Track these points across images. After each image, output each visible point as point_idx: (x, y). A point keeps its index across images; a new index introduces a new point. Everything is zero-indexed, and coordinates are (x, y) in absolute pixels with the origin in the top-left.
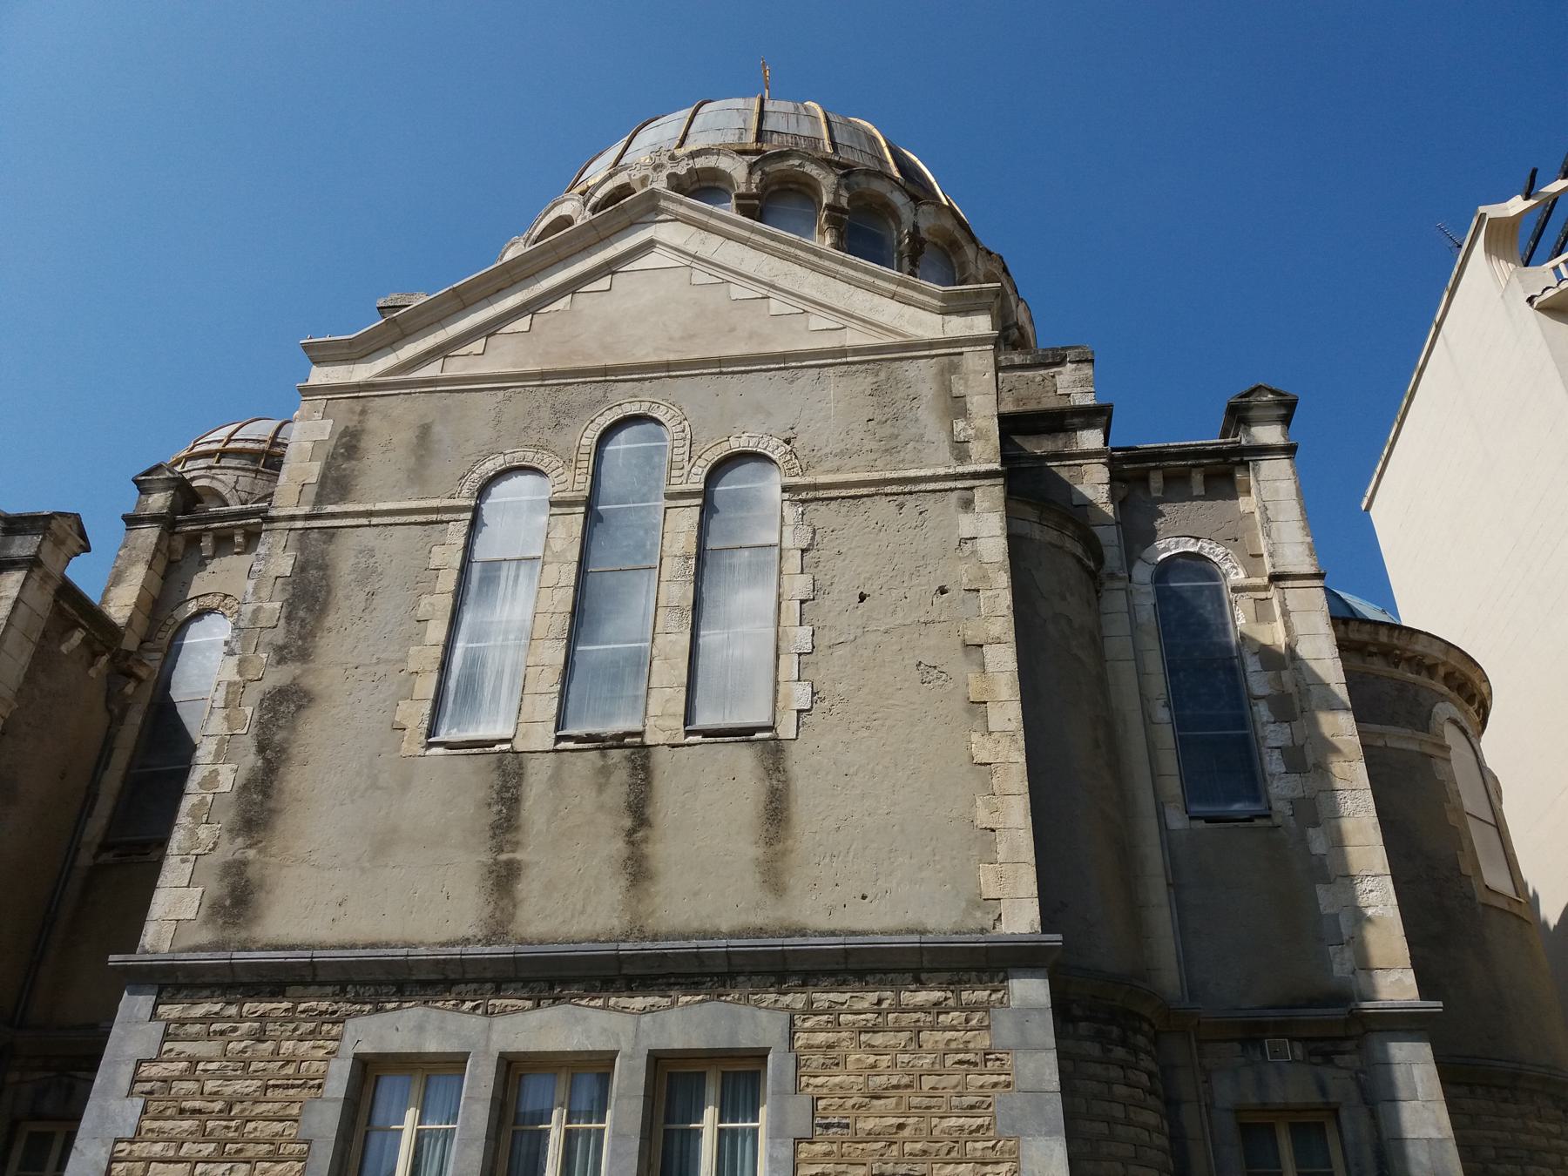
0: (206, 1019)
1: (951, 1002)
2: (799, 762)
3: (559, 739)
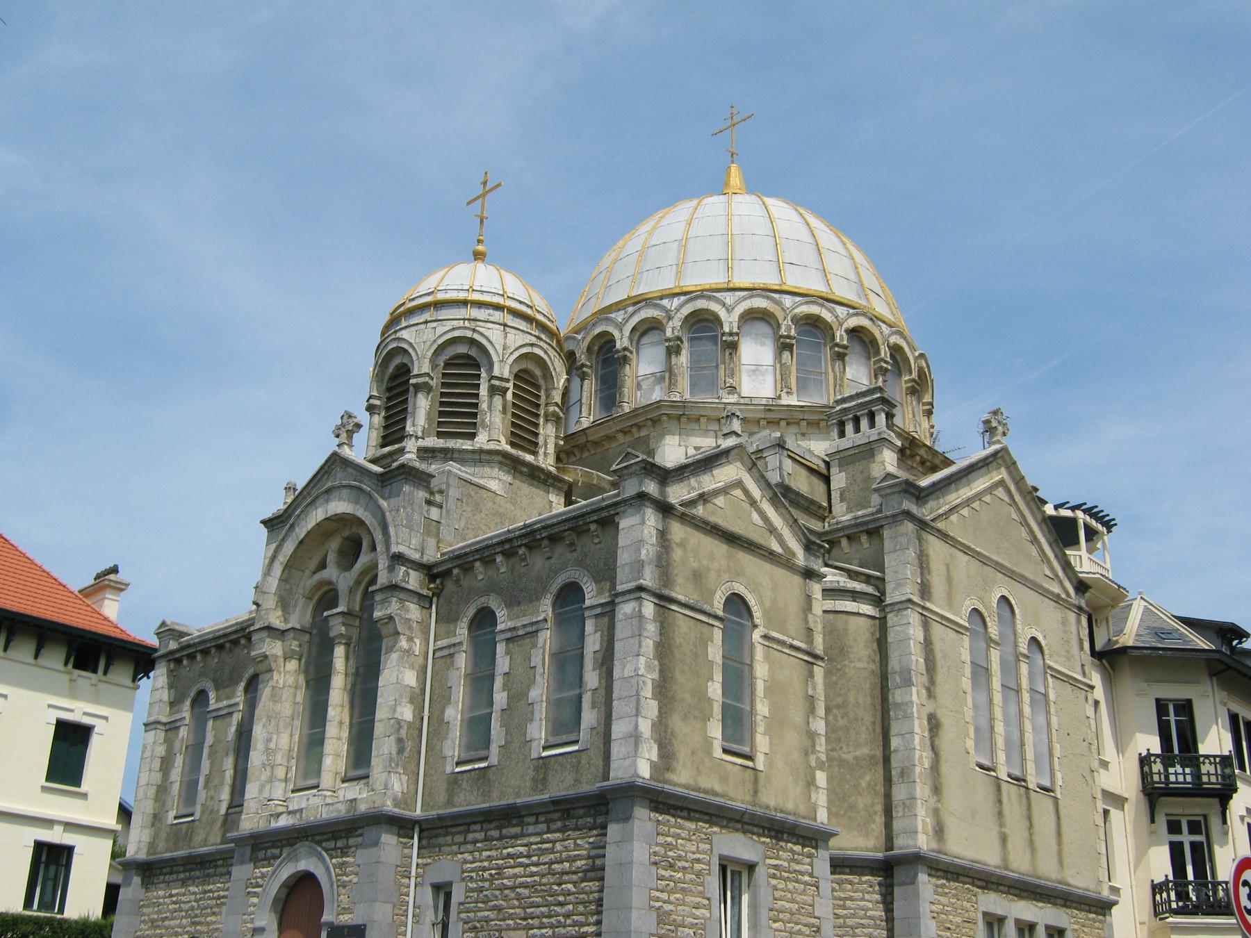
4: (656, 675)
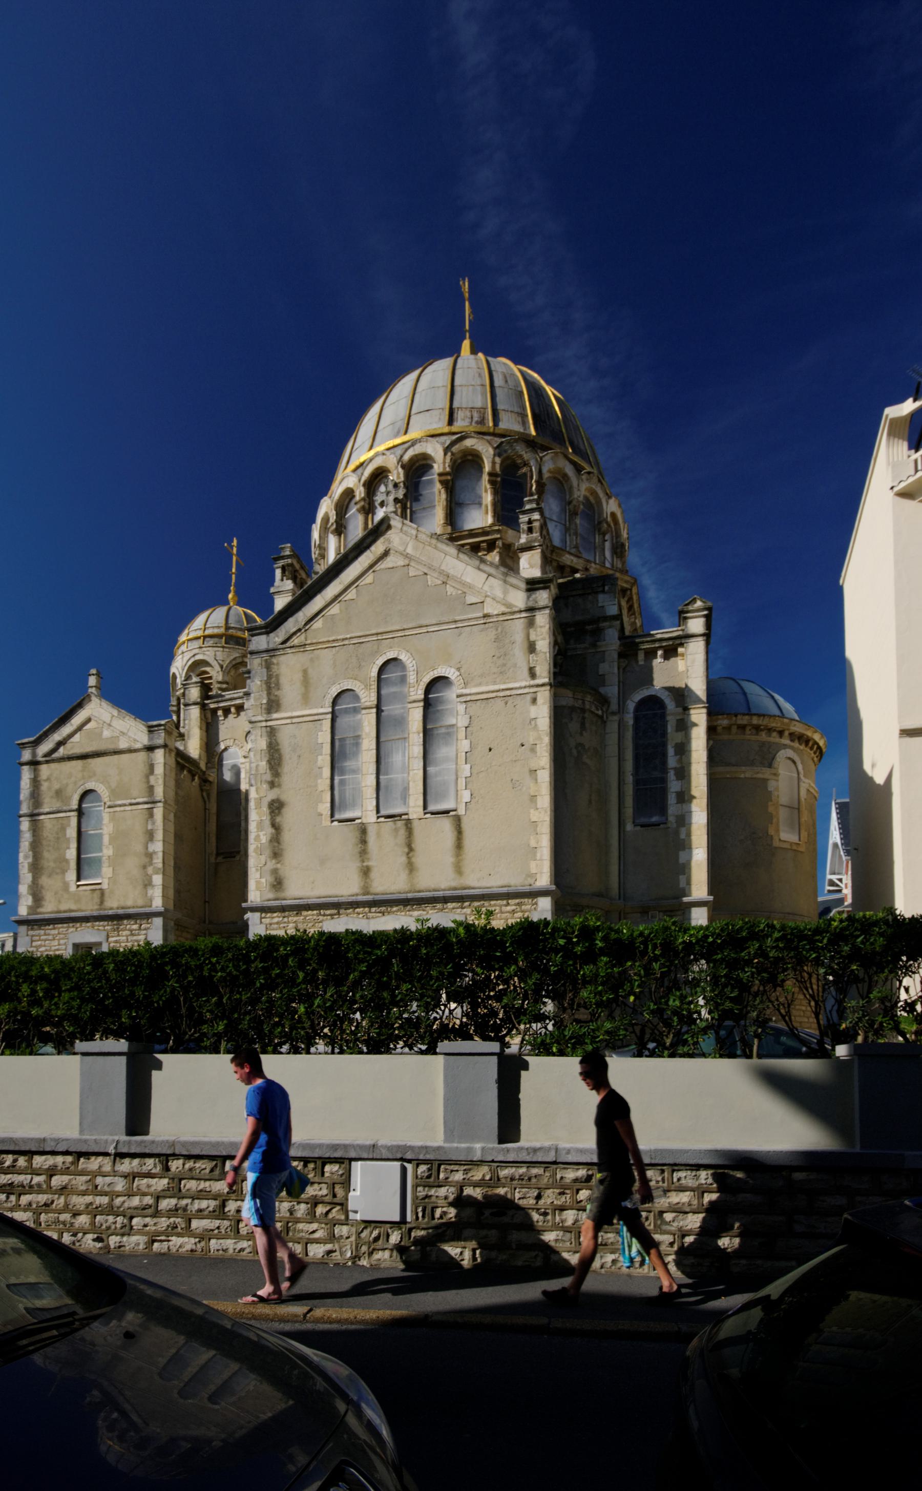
0: (277, 923)
1: (518, 910)
2: (466, 825)
3: (378, 817)
4: (30, 860)
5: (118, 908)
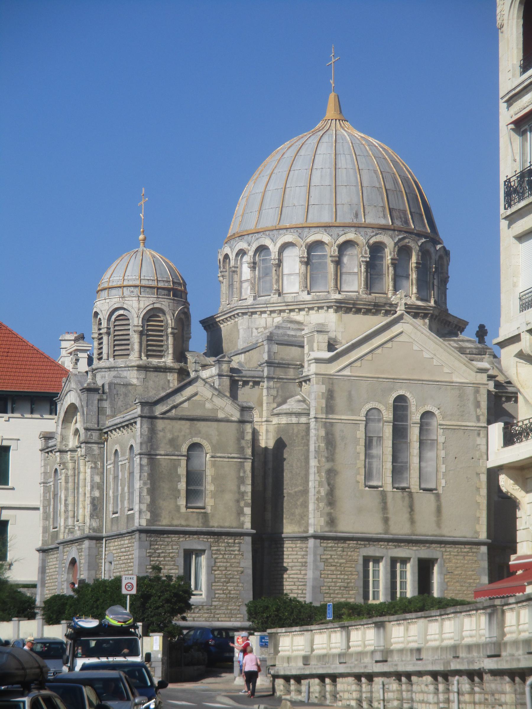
0: (331, 547)
2: (443, 500)
4: (149, 486)
5: (217, 527)
